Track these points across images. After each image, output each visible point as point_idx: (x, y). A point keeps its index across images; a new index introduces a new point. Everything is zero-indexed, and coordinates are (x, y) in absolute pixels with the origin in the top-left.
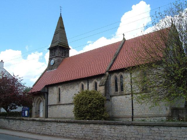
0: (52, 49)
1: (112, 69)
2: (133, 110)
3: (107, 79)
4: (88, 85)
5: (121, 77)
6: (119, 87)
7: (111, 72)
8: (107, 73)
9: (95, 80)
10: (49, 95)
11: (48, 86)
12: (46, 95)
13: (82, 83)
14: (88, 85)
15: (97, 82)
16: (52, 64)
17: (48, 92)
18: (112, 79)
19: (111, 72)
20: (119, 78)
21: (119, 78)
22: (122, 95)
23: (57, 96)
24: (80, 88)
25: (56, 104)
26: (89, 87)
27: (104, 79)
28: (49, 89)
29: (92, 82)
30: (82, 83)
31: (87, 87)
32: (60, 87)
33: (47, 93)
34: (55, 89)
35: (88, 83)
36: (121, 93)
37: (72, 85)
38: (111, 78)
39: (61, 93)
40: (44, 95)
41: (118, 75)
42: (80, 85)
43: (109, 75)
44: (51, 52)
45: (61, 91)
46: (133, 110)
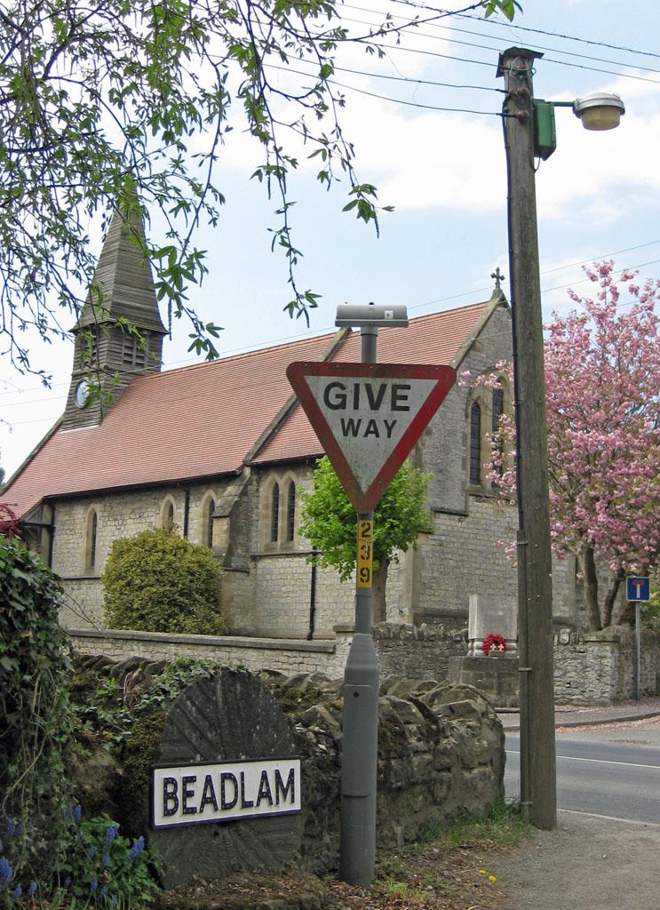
0: (85, 334)
1: (269, 456)
2: (313, 610)
3: (244, 493)
4: (502, 91)
5: (292, 486)
6: (282, 524)
7: (261, 469)
8: (247, 471)
9: (210, 493)
10: (57, 538)
11: (52, 502)
12: (45, 536)
13: (169, 497)
14: (502, 91)
15: (215, 498)
16: (81, 401)
17: (53, 522)
18: (265, 489)
19: (261, 469)
20: (284, 492)
21: (284, 492)
22: (288, 555)
23: (82, 544)
24: (163, 518)
25: (79, 574)
26: (190, 515)
27: (232, 490)
28: (56, 512)
29: (199, 499)
30: (210, 496)
31: (183, 516)
32: (97, 507)
33: (51, 529)
34: (80, 514)
35: (188, 493)
36: (287, 548)
37: (138, 505)
38: (261, 489)
39: (98, 534)
40: (39, 539)
41: (282, 481)
42: (163, 504)
43: (255, 477)
44: (81, 346)
45: (100, 523)
46: (313, 610)
